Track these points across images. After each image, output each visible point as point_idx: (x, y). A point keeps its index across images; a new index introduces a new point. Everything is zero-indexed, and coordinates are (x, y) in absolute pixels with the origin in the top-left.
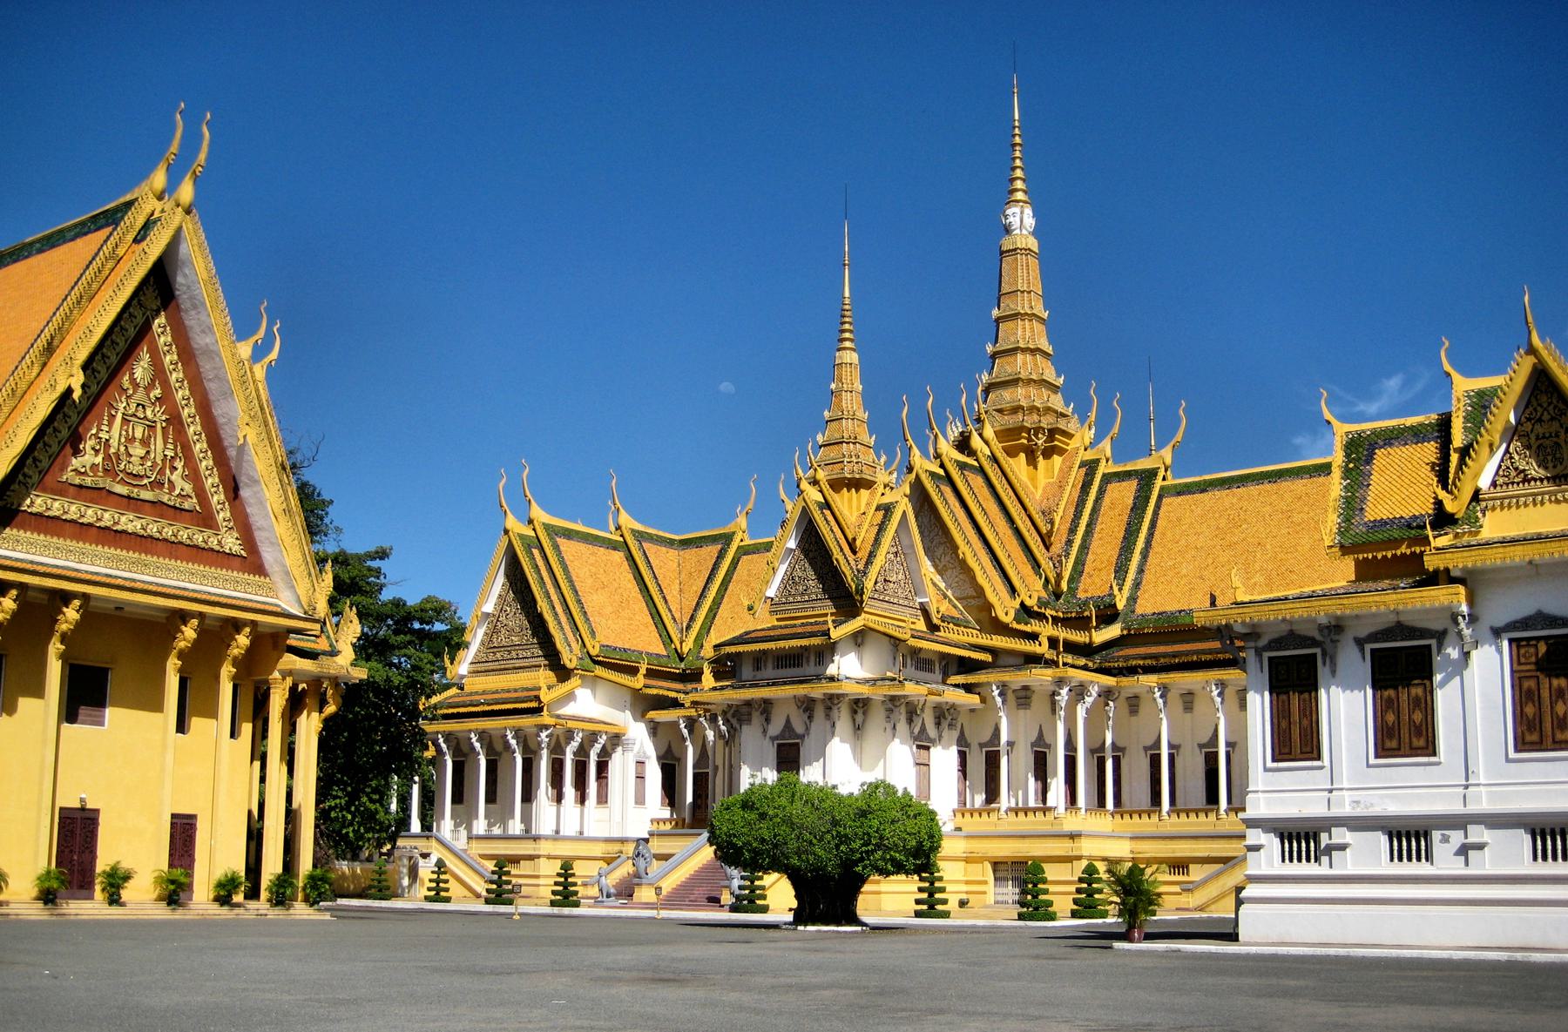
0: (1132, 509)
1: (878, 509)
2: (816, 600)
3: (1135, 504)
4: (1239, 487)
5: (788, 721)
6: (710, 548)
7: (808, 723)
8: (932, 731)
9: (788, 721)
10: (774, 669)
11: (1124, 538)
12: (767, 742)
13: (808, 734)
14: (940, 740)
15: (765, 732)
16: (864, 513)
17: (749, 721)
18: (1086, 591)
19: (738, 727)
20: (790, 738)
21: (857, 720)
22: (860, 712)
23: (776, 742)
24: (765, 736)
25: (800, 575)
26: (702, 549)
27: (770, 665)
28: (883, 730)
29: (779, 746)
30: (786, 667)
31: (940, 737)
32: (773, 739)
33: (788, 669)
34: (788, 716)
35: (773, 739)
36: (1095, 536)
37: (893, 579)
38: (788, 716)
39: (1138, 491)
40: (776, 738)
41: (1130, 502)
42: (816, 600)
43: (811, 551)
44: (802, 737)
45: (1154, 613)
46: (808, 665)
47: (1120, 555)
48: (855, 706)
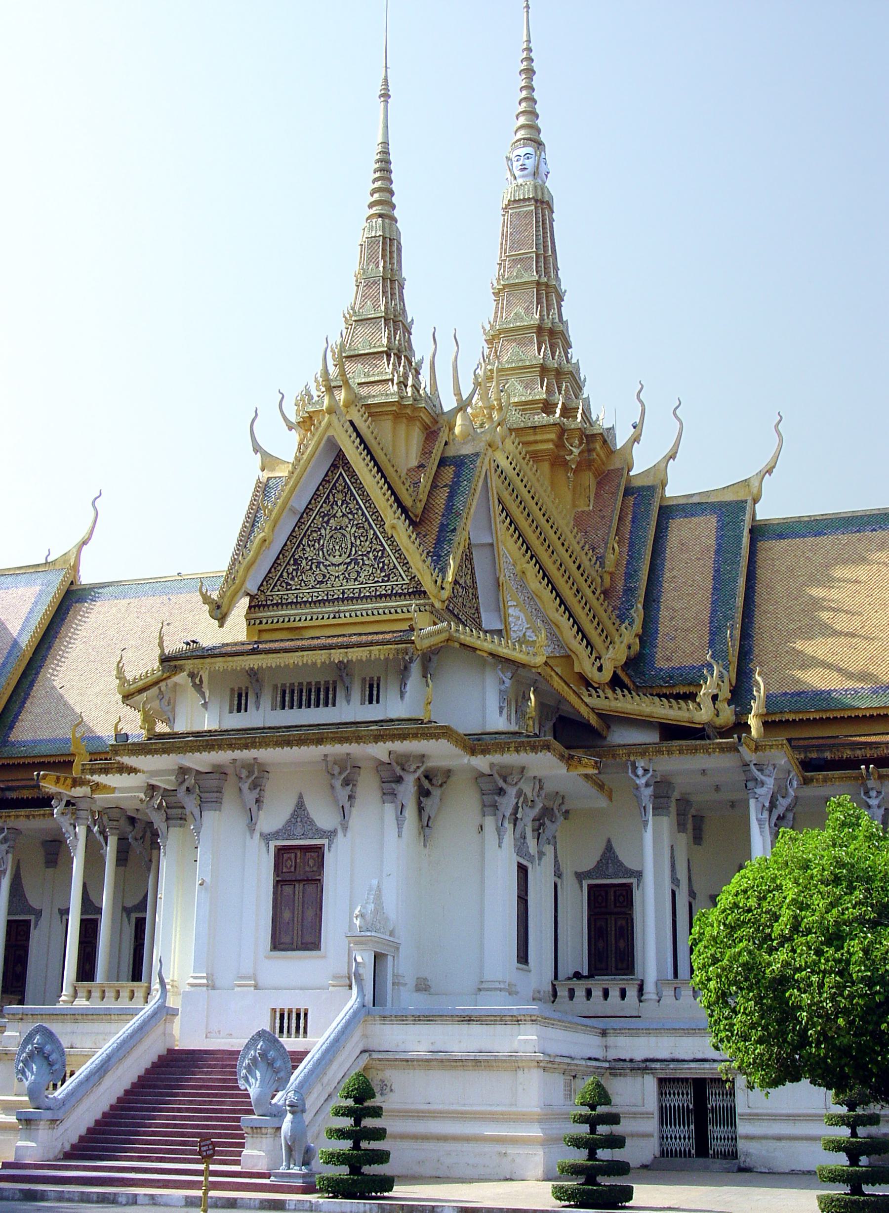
0: (717, 552)
1: (443, 462)
2: (343, 600)
3: (719, 545)
4: (872, 531)
5: (300, 805)
6: (21, 590)
7: (347, 805)
8: (532, 844)
9: (300, 805)
10: (274, 708)
11: (714, 588)
12: (255, 843)
13: (345, 828)
14: (540, 859)
15: (252, 830)
16: (421, 466)
17: (217, 803)
18: (669, 659)
19: (196, 812)
20: (304, 836)
21: (427, 809)
22: (436, 792)
23: (273, 844)
24: (252, 830)
25: (310, 553)
26: (10, 591)
27: (266, 701)
28: (476, 829)
29: (281, 851)
30: (300, 707)
31: (541, 854)
32: (267, 838)
33: (322, 709)
34: (301, 797)
35: (267, 838)
36: (666, 585)
37: (462, 581)
38: (301, 797)
39: (720, 528)
40: (276, 835)
41: (712, 542)
42: (343, 600)
43: (334, 516)
44: (331, 835)
45: (786, 694)
46: (348, 702)
47: (714, 611)
48: (426, 784)
